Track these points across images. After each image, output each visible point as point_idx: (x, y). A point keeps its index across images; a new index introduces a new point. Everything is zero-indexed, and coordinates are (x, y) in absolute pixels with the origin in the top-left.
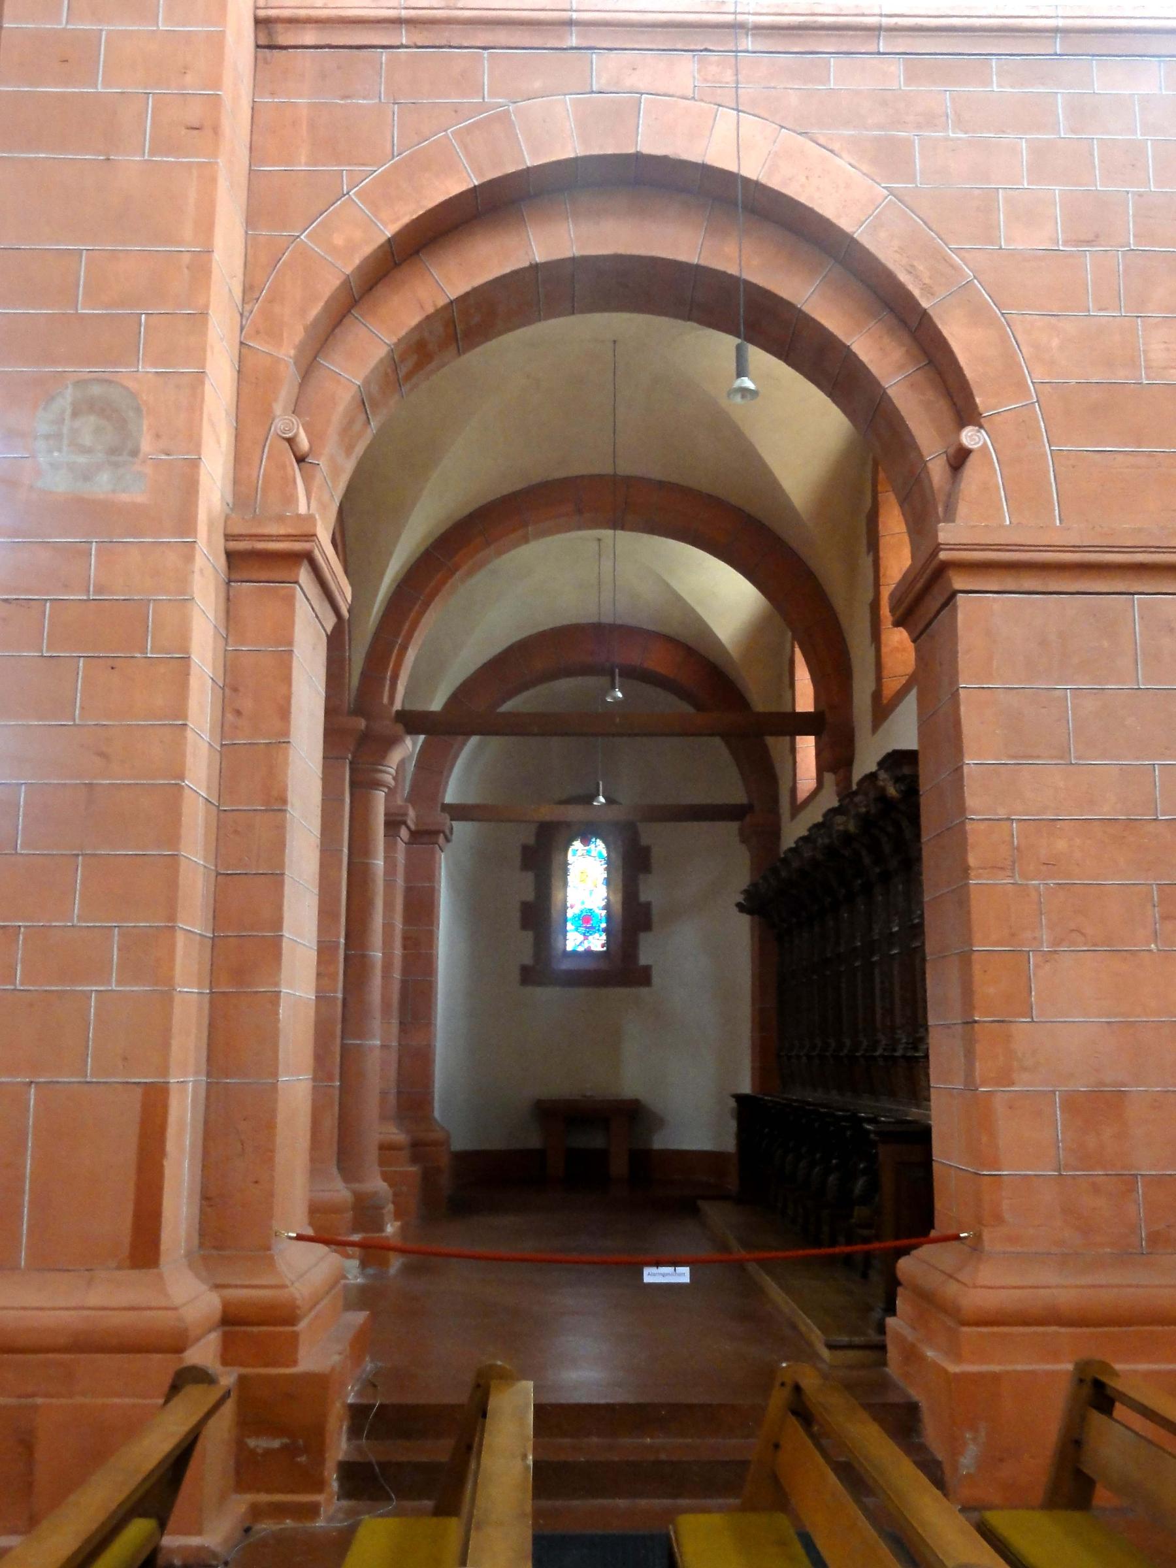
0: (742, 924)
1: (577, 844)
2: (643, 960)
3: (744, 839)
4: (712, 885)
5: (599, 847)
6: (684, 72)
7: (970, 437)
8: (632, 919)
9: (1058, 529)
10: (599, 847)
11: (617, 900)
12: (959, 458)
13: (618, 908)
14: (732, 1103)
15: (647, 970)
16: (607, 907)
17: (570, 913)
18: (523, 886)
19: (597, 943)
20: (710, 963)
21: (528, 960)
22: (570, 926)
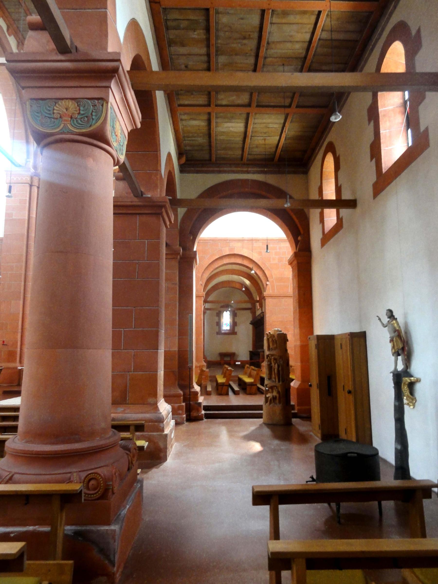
0: (251, 327)
1: (225, 312)
2: (236, 331)
3: (251, 313)
4: (246, 320)
5: (228, 313)
6: (239, 244)
7: (268, 283)
8: (234, 324)
9: (276, 293)
10: (228, 313)
11: (232, 321)
12: (267, 285)
13: (232, 322)
14: (249, 353)
15: (236, 332)
16: (230, 322)
17: (224, 324)
18: (217, 319)
19: (228, 328)
20: (246, 331)
21: (217, 331)
22: (224, 325)
